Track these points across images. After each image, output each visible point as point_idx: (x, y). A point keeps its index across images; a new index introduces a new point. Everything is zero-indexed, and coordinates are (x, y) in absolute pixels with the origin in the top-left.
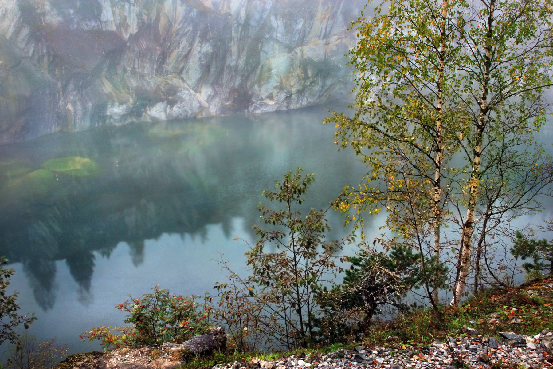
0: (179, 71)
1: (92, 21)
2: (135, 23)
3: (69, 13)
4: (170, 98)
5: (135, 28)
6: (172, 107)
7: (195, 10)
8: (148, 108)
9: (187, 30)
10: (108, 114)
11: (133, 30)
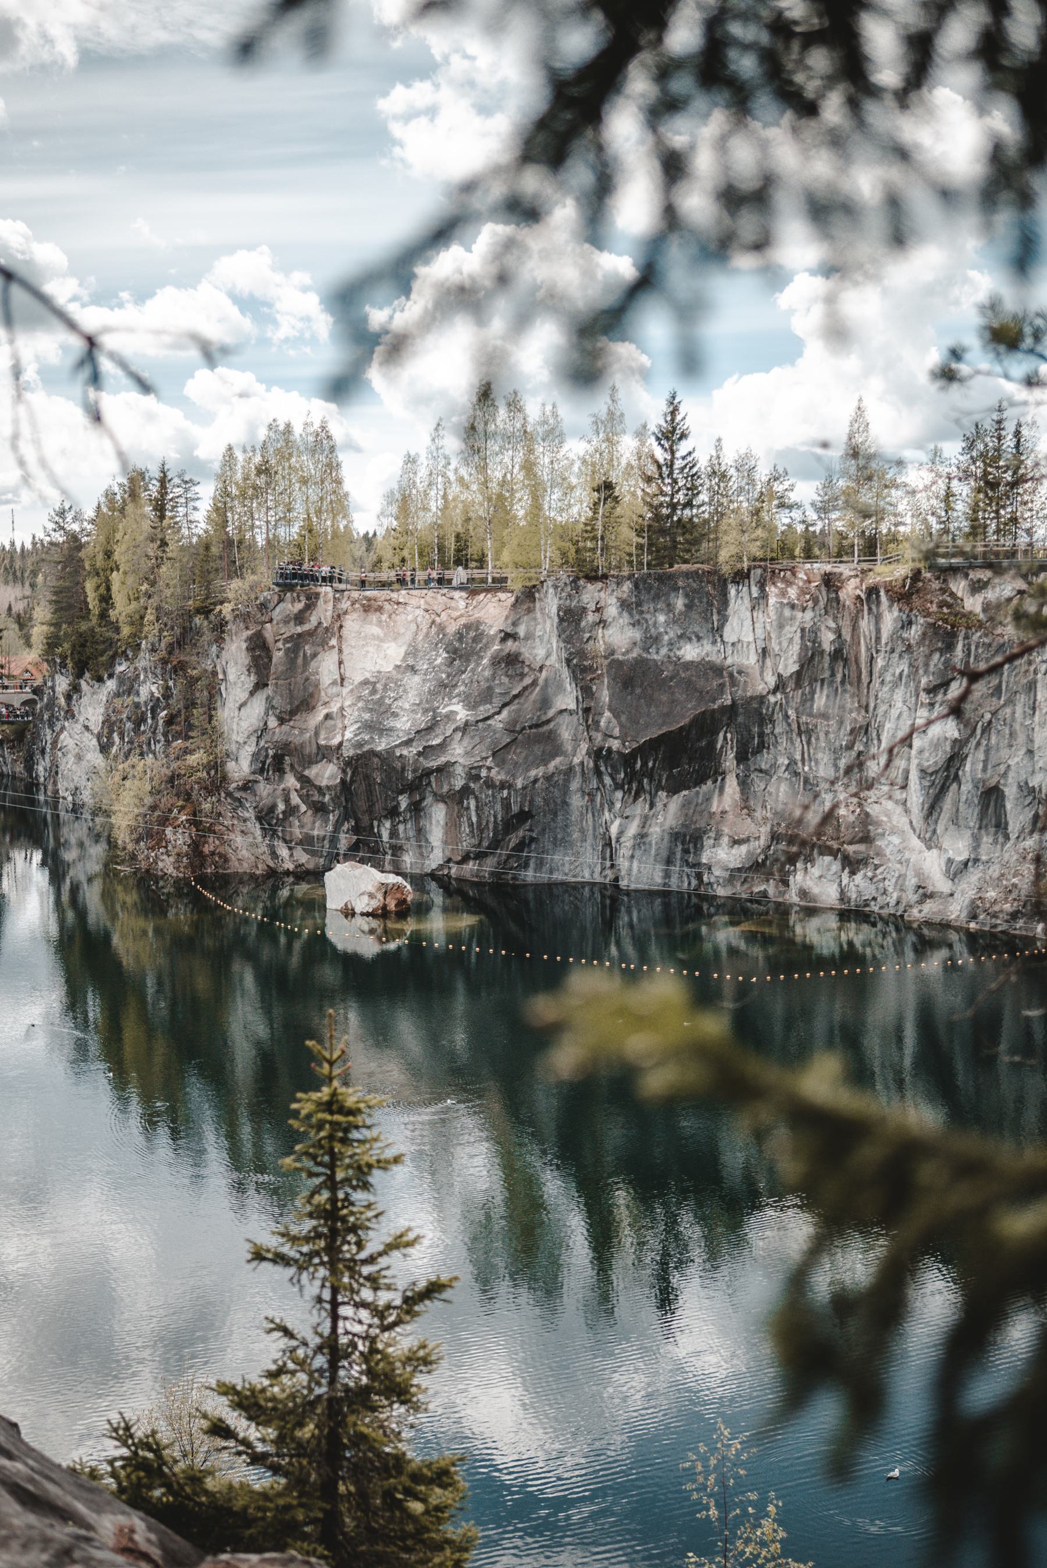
0: (900, 781)
1: (705, 642)
2: (796, 648)
3: (655, 623)
4: (851, 849)
5: (791, 661)
6: (853, 873)
7: (921, 620)
8: (799, 865)
9: (898, 672)
10: (704, 861)
11: (786, 666)
